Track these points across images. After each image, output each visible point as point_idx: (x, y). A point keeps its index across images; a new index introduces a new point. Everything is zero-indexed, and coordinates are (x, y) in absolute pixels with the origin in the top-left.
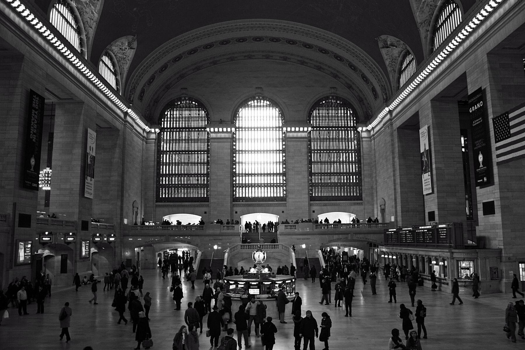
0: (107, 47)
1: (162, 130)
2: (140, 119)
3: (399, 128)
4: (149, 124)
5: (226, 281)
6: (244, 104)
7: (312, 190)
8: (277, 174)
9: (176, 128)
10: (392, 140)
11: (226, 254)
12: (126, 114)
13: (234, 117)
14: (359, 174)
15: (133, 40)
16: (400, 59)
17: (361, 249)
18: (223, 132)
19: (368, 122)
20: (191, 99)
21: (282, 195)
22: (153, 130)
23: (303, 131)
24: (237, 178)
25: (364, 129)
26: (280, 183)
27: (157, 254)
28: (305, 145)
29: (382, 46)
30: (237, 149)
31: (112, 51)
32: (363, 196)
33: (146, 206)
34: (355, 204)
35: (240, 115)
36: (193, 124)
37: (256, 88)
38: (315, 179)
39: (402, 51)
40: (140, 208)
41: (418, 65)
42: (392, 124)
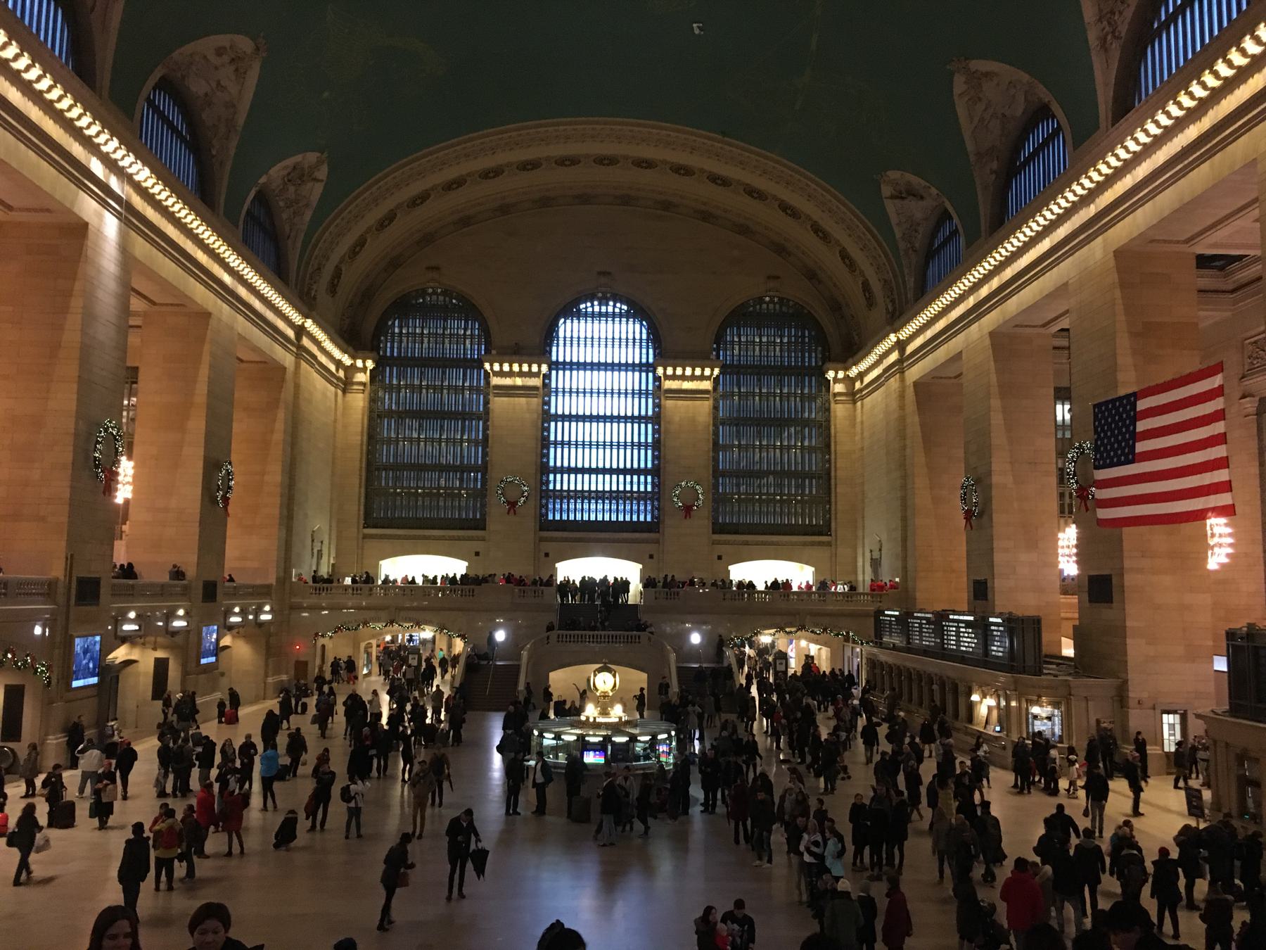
0: (263, 180)
2: (332, 340)
3: (916, 384)
4: (350, 349)
8: (638, 472)
9: (413, 358)
10: (902, 407)
11: (525, 654)
12: (300, 331)
13: (546, 338)
17: (825, 644)
19: (850, 360)
20: (445, 293)
22: (359, 363)
23: (702, 378)
24: (551, 477)
25: (841, 375)
27: (363, 645)
28: (705, 406)
29: (888, 194)
30: (553, 411)
33: (339, 538)
34: (813, 544)
35: (561, 334)
37: (600, 273)
40: (326, 542)
42: (902, 372)
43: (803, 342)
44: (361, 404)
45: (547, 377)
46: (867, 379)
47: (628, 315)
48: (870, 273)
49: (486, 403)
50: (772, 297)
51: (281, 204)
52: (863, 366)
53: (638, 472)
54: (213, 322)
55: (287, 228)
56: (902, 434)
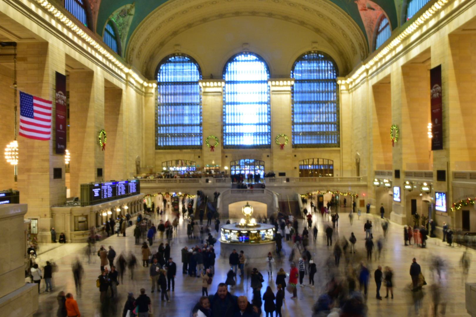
4: (147, 80)
5: (222, 230)
6: (232, 60)
7: (294, 138)
8: (262, 124)
12: (127, 74)
15: (132, 7)
19: (347, 76)
20: (183, 55)
21: (267, 143)
22: (150, 85)
23: (287, 86)
24: (227, 127)
26: (265, 133)
30: (227, 101)
35: (229, 70)
36: (187, 78)
42: (368, 81)
43: (328, 70)
45: (224, 87)
47: (256, 60)
48: (354, 41)
49: (200, 98)
51: (118, 25)
53: (262, 124)
55: (120, 34)
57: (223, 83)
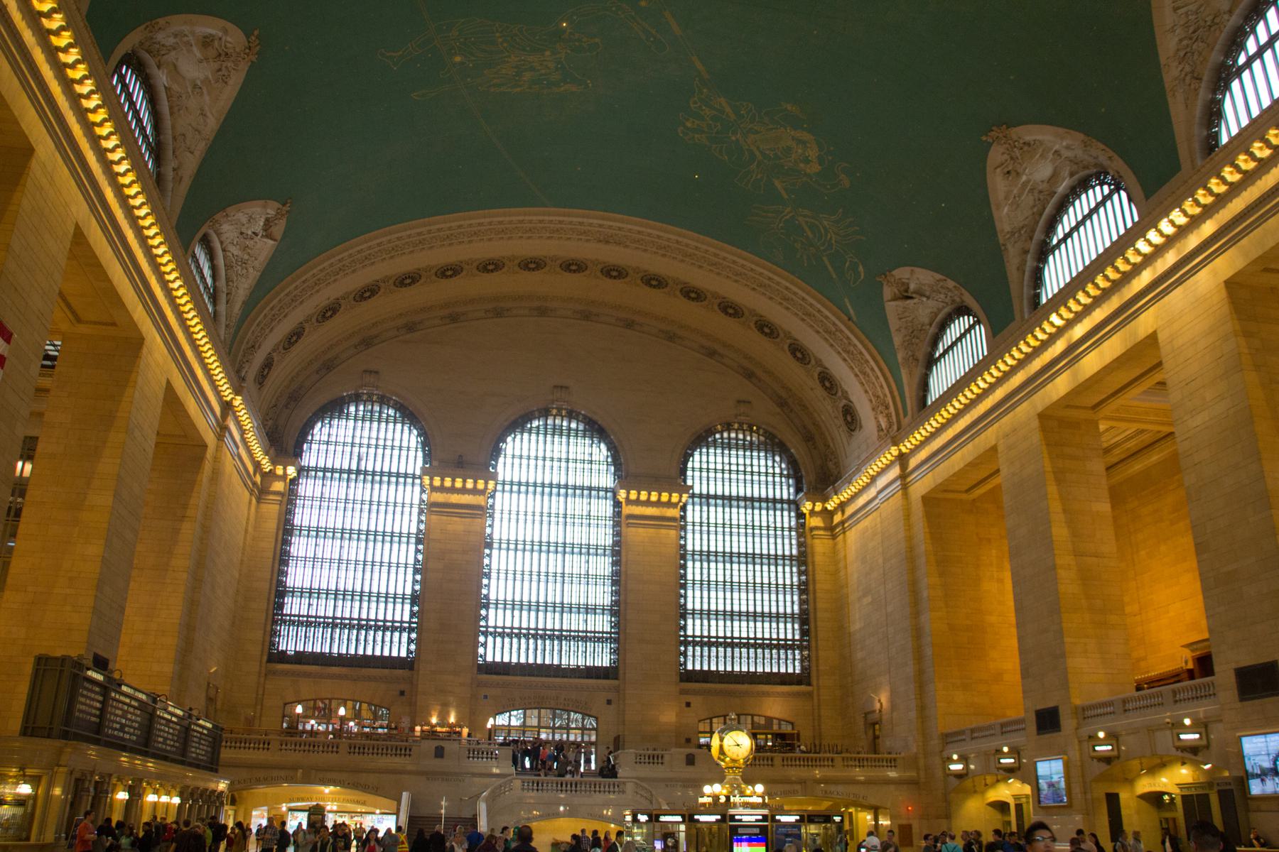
1: (302, 471)
3: (926, 499)
4: (272, 451)
6: (518, 424)
10: (909, 526)
12: (227, 407)
14: (804, 619)
16: (933, 330)
18: (464, 491)
20: (383, 401)
22: (279, 470)
23: (669, 504)
24: (492, 612)
25: (819, 507)
31: (219, 235)
32: (814, 674)
38: (694, 627)
39: (940, 310)
41: (994, 335)
42: (905, 487)
44: (276, 516)
46: (850, 510)
50: (741, 424)
52: (844, 496)
54: (145, 350)
56: (910, 557)
57: (491, 484)
